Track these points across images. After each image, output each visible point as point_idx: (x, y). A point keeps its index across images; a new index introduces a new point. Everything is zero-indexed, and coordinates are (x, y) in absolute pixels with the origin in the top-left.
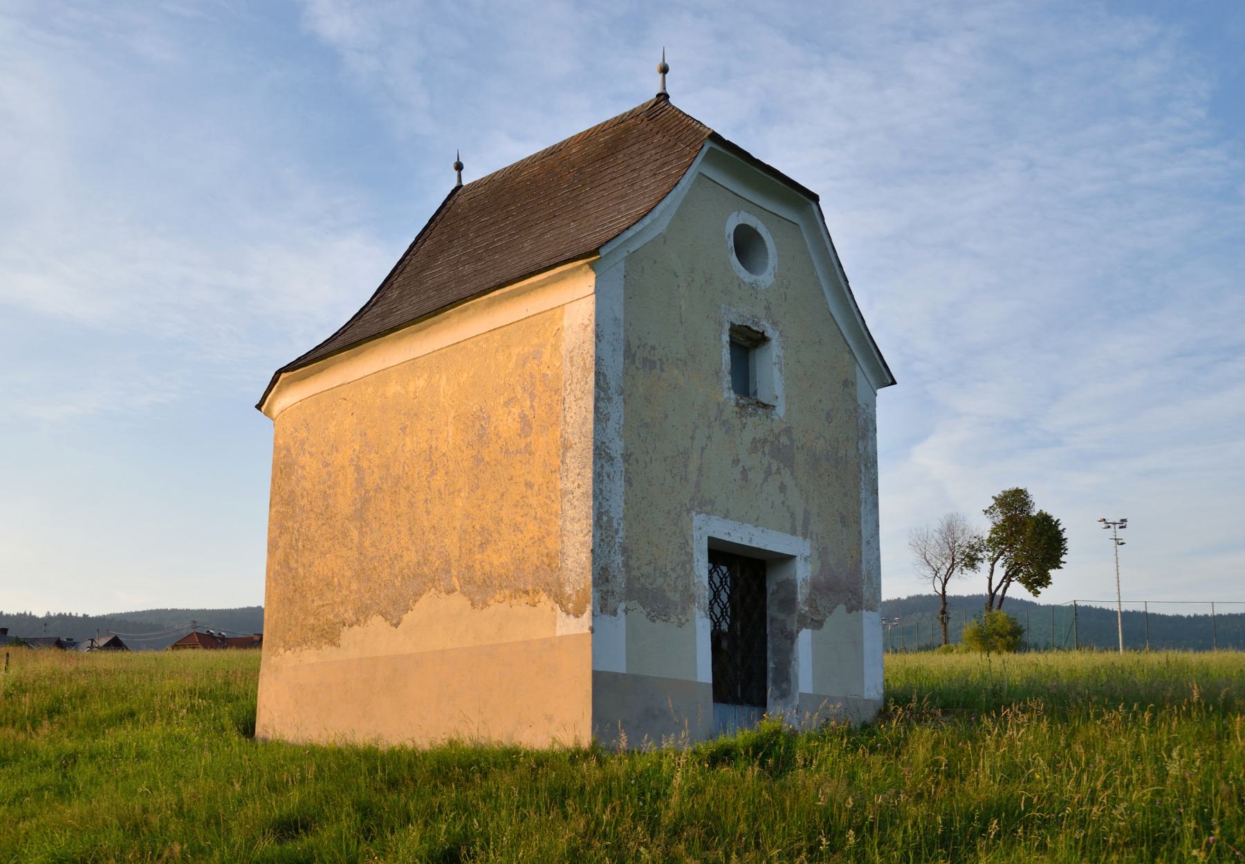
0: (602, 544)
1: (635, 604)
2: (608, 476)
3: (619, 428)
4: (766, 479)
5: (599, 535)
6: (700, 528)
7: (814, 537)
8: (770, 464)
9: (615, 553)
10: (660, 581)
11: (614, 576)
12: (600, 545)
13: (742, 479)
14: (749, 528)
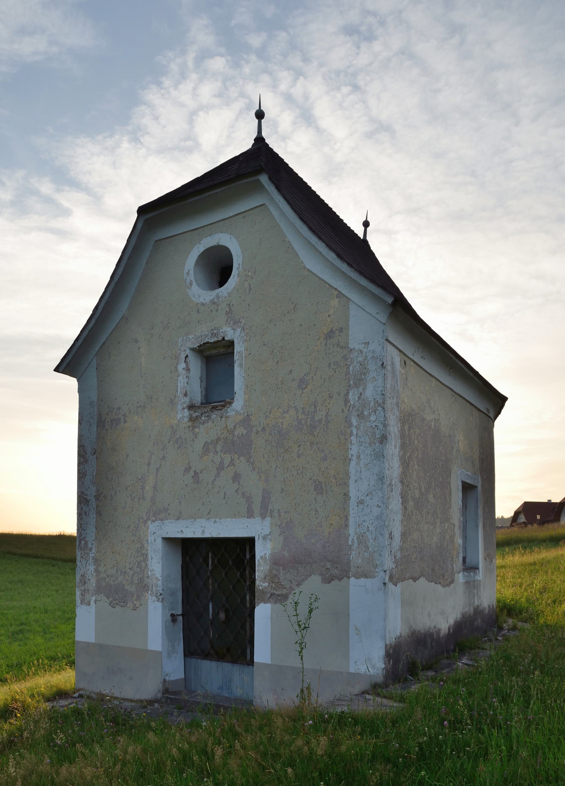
0: (81, 559)
1: (102, 597)
2: (86, 514)
3: (93, 478)
4: (218, 474)
5: (80, 554)
6: (154, 533)
7: (276, 514)
8: (222, 459)
9: (89, 564)
10: (120, 578)
11: (89, 580)
12: (80, 560)
13: (194, 482)
14: (202, 522)
